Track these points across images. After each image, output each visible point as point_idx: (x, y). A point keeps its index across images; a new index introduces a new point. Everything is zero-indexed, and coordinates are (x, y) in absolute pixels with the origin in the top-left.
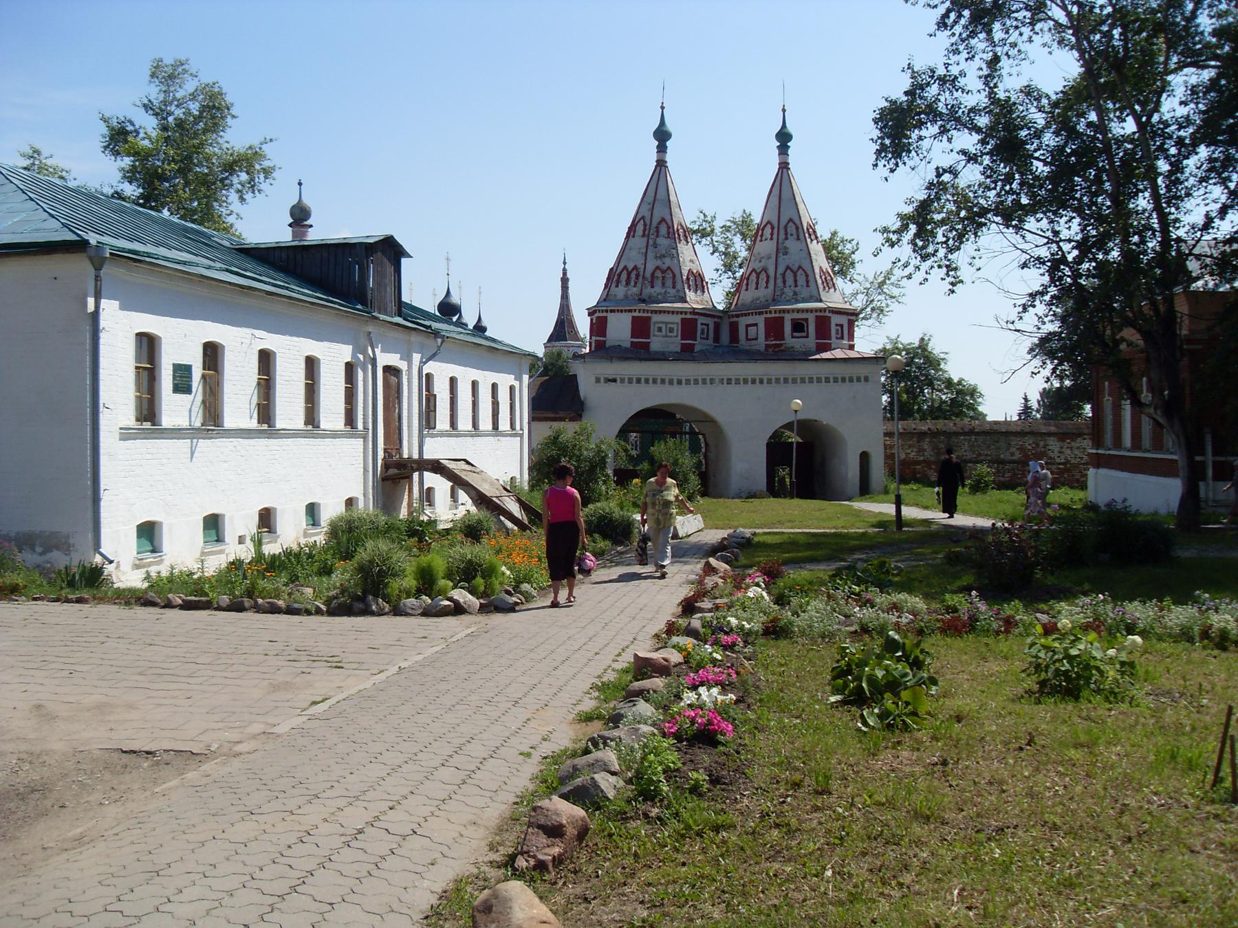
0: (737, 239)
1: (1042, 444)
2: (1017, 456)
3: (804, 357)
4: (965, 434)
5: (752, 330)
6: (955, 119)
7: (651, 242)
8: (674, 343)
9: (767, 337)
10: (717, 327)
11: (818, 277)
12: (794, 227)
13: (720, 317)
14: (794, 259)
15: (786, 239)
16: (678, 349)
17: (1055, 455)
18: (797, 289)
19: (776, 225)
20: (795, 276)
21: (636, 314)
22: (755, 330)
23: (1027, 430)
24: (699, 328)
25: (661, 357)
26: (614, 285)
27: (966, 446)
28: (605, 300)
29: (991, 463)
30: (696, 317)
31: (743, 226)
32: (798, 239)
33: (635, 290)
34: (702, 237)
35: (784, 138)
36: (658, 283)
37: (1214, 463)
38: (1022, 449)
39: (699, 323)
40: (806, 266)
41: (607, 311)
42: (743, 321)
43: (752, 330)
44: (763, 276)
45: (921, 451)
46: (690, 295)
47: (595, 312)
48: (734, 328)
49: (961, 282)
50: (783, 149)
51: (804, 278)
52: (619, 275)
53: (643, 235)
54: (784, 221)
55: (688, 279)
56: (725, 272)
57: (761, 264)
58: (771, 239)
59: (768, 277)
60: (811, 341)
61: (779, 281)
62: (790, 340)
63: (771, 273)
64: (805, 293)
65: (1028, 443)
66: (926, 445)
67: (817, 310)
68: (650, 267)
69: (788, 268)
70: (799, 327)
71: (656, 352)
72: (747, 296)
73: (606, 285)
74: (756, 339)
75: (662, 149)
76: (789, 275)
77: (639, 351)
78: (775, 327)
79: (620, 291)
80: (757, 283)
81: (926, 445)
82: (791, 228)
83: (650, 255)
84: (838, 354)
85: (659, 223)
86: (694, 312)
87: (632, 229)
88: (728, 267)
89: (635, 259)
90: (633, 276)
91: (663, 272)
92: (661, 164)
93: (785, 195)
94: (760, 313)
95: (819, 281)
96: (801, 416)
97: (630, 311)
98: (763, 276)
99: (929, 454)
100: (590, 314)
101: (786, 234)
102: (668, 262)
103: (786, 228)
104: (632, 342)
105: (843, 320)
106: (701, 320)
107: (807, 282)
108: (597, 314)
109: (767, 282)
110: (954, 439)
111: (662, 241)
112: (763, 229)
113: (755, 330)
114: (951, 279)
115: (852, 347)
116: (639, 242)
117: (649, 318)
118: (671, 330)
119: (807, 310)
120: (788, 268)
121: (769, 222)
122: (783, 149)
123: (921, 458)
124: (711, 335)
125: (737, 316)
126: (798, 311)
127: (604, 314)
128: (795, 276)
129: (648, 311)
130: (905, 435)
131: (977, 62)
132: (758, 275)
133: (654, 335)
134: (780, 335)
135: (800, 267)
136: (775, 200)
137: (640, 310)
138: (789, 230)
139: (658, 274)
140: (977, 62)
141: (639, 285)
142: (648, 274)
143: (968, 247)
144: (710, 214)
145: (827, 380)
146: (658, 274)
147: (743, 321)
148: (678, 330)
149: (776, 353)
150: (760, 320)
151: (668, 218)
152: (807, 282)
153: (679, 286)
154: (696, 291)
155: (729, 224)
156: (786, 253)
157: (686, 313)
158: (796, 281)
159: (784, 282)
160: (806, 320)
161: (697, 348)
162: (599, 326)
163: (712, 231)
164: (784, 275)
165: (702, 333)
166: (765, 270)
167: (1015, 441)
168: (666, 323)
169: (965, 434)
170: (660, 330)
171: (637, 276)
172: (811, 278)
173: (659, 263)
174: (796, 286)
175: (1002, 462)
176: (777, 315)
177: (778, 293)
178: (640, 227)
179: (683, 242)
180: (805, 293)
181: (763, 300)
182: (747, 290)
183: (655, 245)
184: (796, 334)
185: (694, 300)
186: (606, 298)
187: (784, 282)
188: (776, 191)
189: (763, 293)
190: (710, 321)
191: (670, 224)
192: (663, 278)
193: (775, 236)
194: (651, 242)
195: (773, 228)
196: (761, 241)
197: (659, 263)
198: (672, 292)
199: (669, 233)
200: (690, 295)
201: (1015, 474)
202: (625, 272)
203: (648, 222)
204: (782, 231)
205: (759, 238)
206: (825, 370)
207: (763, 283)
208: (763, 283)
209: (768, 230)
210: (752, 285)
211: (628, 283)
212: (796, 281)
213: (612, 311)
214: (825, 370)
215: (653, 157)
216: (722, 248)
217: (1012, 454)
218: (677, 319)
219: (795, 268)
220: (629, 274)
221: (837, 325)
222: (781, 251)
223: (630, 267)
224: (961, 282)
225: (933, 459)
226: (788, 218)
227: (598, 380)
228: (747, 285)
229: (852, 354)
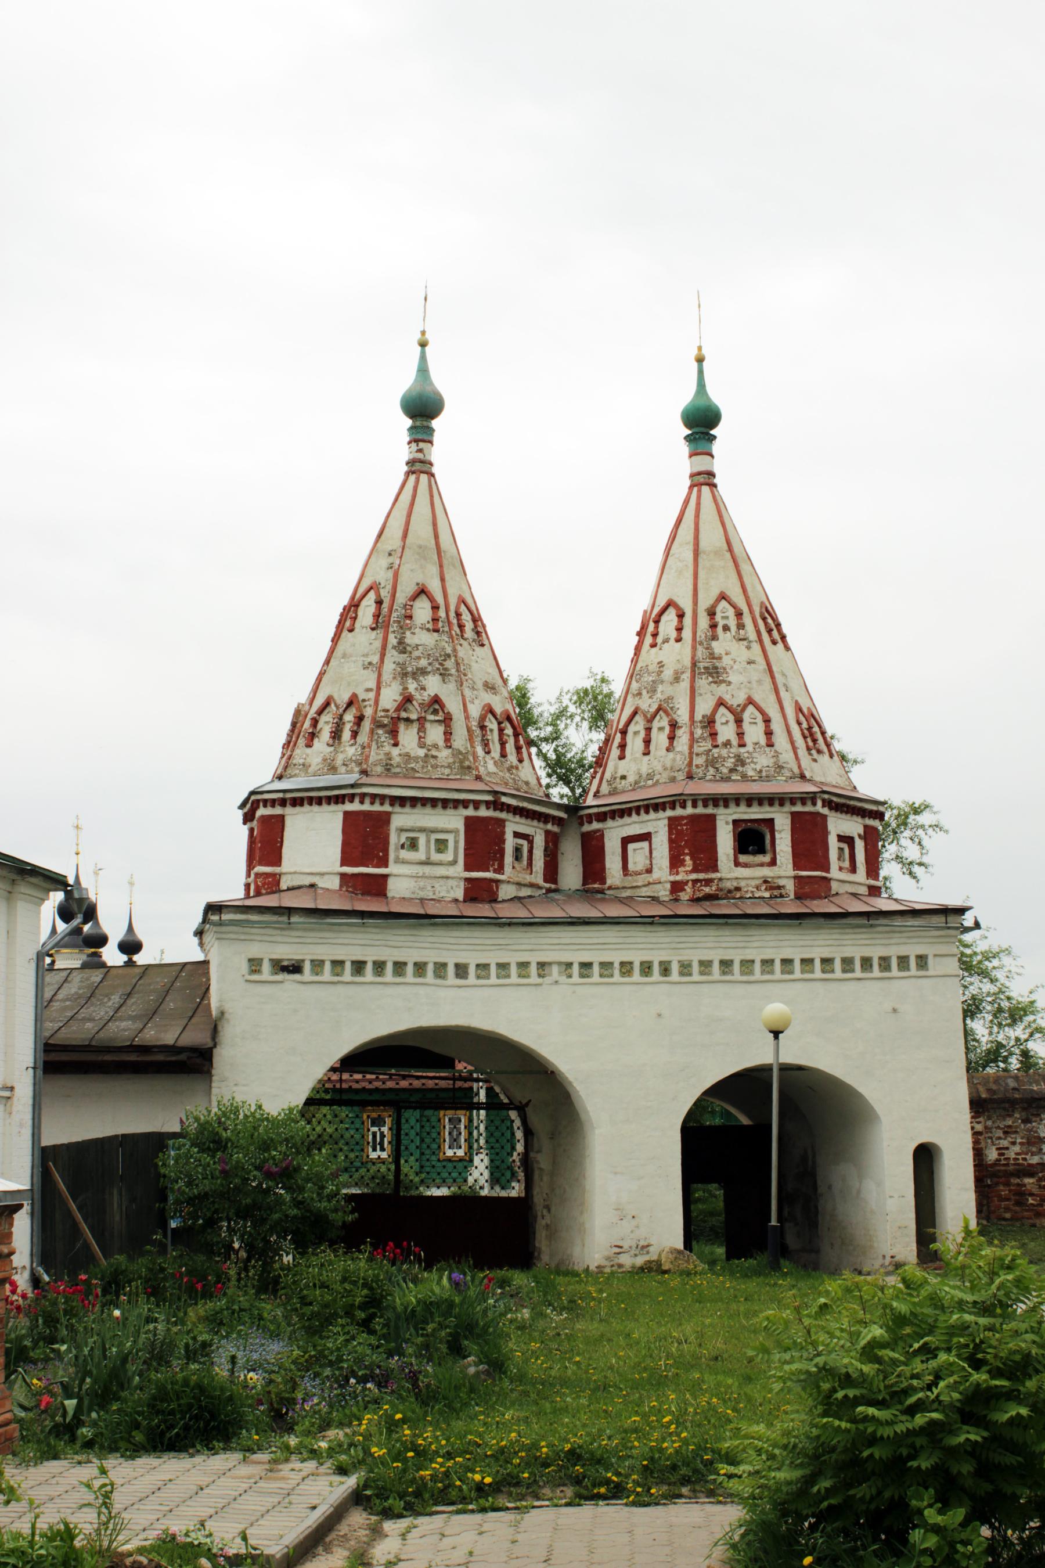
5: (638, 854)
7: (392, 640)
12: (731, 612)
13: (559, 821)
16: (460, 894)
19: (687, 606)
20: (739, 721)
21: (355, 806)
24: (510, 843)
26: (302, 742)
30: (503, 815)
39: (510, 829)
41: (283, 803)
42: (614, 833)
44: (662, 721)
51: (761, 727)
54: (705, 601)
58: (678, 640)
59: (674, 725)
63: (682, 715)
69: (721, 703)
80: (647, 742)
83: (389, 667)
85: (415, 597)
87: (351, 610)
98: (662, 721)
103: (711, 613)
104: (343, 876)
105: (853, 826)
106: (514, 825)
112: (657, 622)
117: (384, 819)
121: (670, 604)
123: (1035, 1160)
125: (602, 817)
127: (278, 811)
128: (739, 721)
129: (382, 798)
133: (398, 861)
134: (707, 860)
135: (750, 701)
136: (683, 552)
138: (718, 618)
141: (363, 738)
148: (457, 845)
157: (477, 804)
160: (770, 822)
161: (505, 892)
165: (518, 851)
174: (742, 745)
176: (700, 810)
182: (622, 757)
183: (402, 647)
184: (743, 858)
188: (686, 532)
191: (440, 599)
193: (687, 634)
194: (392, 640)
195: (681, 616)
196: (653, 645)
199: (435, 620)
203: (385, 594)
204: (704, 622)
205: (649, 640)
207: (660, 739)
208: (660, 739)
209: (670, 619)
210: (635, 744)
211: (336, 735)
215: (402, 452)
221: (841, 838)
223: (343, 698)
226: (715, 593)
227: (255, 965)
228: (623, 746)
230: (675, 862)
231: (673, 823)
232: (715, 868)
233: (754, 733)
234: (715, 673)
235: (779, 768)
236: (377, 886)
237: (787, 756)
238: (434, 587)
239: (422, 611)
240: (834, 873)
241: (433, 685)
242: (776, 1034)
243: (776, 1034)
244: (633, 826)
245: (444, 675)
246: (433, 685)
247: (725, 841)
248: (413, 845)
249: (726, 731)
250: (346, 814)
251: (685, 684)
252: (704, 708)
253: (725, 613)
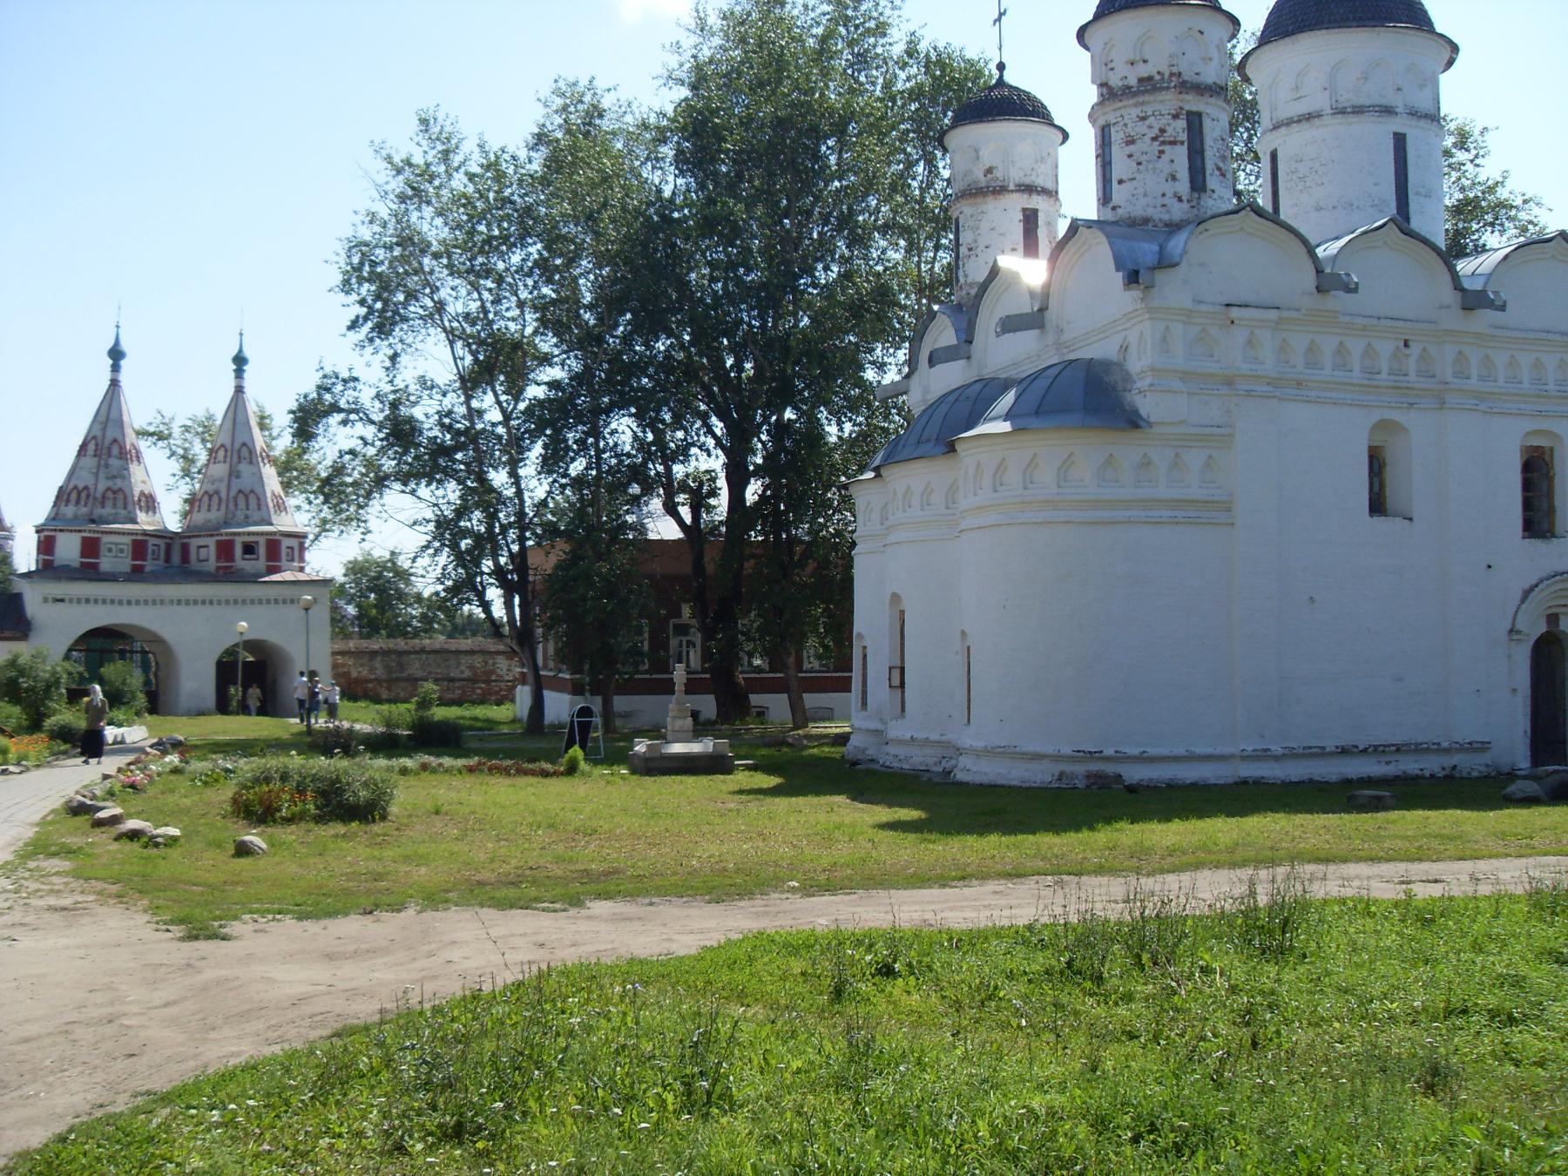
0: (197, 441)
1: (491, 662)
2: (467, 674)
3: (252, 579)
4: (416, 652)
5: (203, 552)
6: (355, 411)
7: (103, 462)
8: (125, 564)
9: (219, 558)
10: (169, 547)
11: (269, 500)
14: (245, 483)
15: (239, 462)
17: (504, 673)
18: (249, 512)
19: (229, 447)
22: (206, 552)
23: (477, 649)
24: (150, 549)
25: (111, 578)
27: (417, 665)
28: (54, 519)
29: (436, 681)
31: (204, 429)
32: (251, 463)
33: (84, 510)
34: (159, 439)
35: (240, 361)
36: (109, 503)
38: (471, 667)
40: (258, 490)
42: (194, 543)
44: (215, 499)
45: (372, 670)
46: (141, 516)
47: (42, 531)
48: (185, 549)
49: (370, 532)
50: (239, 373)
52: (69, 494)
53: (95, 456)
54: (237, 445)
55: (140, 500)
56: (183, 477)
57: (214, 487)
59: (220, 499)
60: (261, 564)
61: (231, 506)
63: (223, 495)
64: (256, 516)
66: (378, 663)
67: (267, 533)
68: (101, 487)
70: (249, 549)
72: (199, 517)
73: (55, 504)
74: (207, 560)
75: (116, 368)
76: (241, 501)
77: (88, 571)
78: (225, 549)
79: (69, 511)
81: (378, 663)
82: (245, 452)
83: (102, 475)
84: (287, 576)
86: (145, 533)
87: (83, 448)
88: (186, 473)
89: (85, 479)
90: (83, 495)
91: (115, 492)
92: (114, 383)
93: (240, 418)
94: (211, 535)
95: (271, 505)
96: (245, 638)
97: (80, 531)
99: (380, 672)
100: (37, 532)
101: (239, 457)
102: (119, 483)
103: (239, 451)
105: (294, 543)
106: (152, 541)
107: (259, 505)
108: (46, 533)
109: (219, 505)
110: (405, 658)
111: (114, 462)
113: (206, 552)
114: (362, 530)
115: (302, 569)
116: (89, 461)
118: (122, 551)
119: (257, 534)
120: (240, 491)
121: (222, 446)
122: (239, 373)
124: (162, 556)
125: (189, 537)
126: (249, 534)
130: (358, 654)
131: (381, 356)
132: (210, 497)
137: (90, 530)
139: (110, 495)
140: (381, 356)
141: (89, 505)
142: (99, 495)
143: (375, 505)
144: (168, 415)
146: (110, 495)
147: (194, 543)
148: (128, 550)
149: (227, 575)
150: (211, 542)
151: (119, 438)
152: (259, 505)
153: (130, 508)
154: (147, 512)
155: (189, 423)
156: (238, 477)
158: (247, 505)
159: (236, 505)
161: (148, 569)
162: (46, 545)
163: (170, 435)
164: (235, 499)
166: (217, 492)
167: (464, 660)
168: (117, 544)
169: (416, 652)
171: (88, 496)
172: (262, 503)
173: (110, 484)
175: (451, 680)
177: (230, 516)
178: (91, 447)
179: (136, 463)
180: (256, 516)
181: (214, 522)
183: (107, 466)
184: (247, 556)
185: (145, 522)
186: (55, 517)
187: (236, 505)
189: (215, 515)
190: (161, 542)
192: (115, 499)
194: (103, 462)
195: (226, 451)
197: (110, 484)
198: (123, 512)
200: (141, 516)
201: (464, 692)
202: (75, 492)
204: (235, 456)
206: (273, 592)
207: (215, 506)
208: (215, 506)
211: (78, 503)
212: (247, 505)
213: (61, 531)
214: (273, 592)
216: (181, 452)
217: (462, 672)
218: (127, 540)
219: (247, 491)
220: (79, 493)
222: (234, 474)
223: (81, 486)
224: (370, 532)
225: (384, 677)
227: (46, 600)
229: (301, 577)
232: (233, 561)
236: (95, 566)
242: (307, 609)
243: (307, 609)
244: (202, 541)
247: (238, 550)
250: (84, 538)
251: (225, 483)
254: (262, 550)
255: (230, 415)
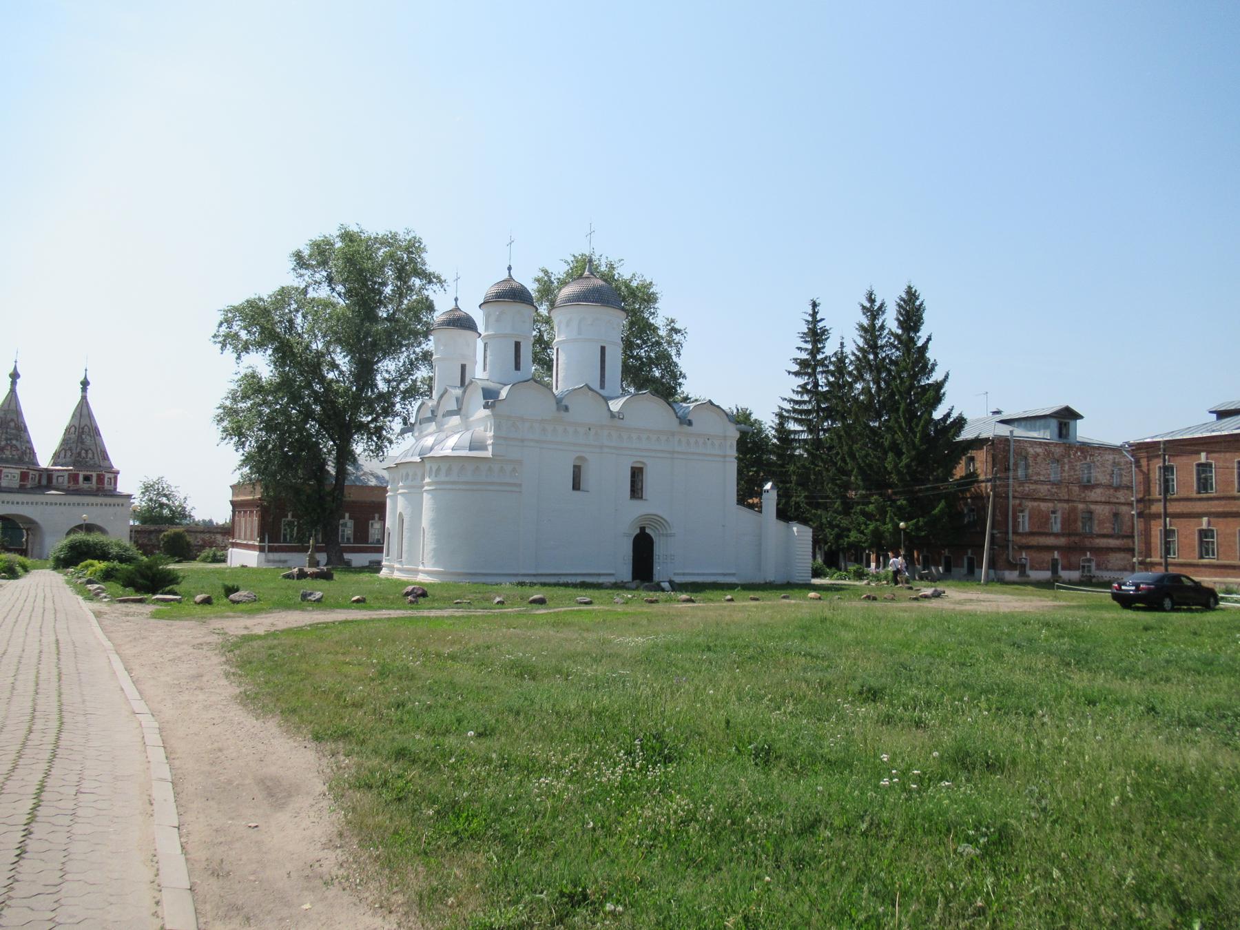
2: (201, 543)
8: (16, 483)
10: (40, 476)
37: (269, 546)
43: (60, 479)
62: (82, 483)
63: (74, 452)
65: (207, 536)
66: (152, 537)
71: (5, 488)
75: (14, 383)
103: (83, 428)
106: (31, 472)
118: (14, 477)
145: (101, 505)
148: (18, 477)
167: (200, 536)
170: (7, 476)
183: (7, 433)
230: (69, 482)
231: (69, 474)
233: (90, 455)
234: (82, 443)
235: (95, 464)
237: (97, 462)
238: (16, 419)
239: (12, 424)
240: (106, 485)
241: (14, 442)
245: (17, 440)
246: (14, 442)
247: (81, 479)
248: (7, 476)
249: (83, 454)
252: (78, 450)
253: (86, 429)
254: (94, 479)
255: (79, 410)
